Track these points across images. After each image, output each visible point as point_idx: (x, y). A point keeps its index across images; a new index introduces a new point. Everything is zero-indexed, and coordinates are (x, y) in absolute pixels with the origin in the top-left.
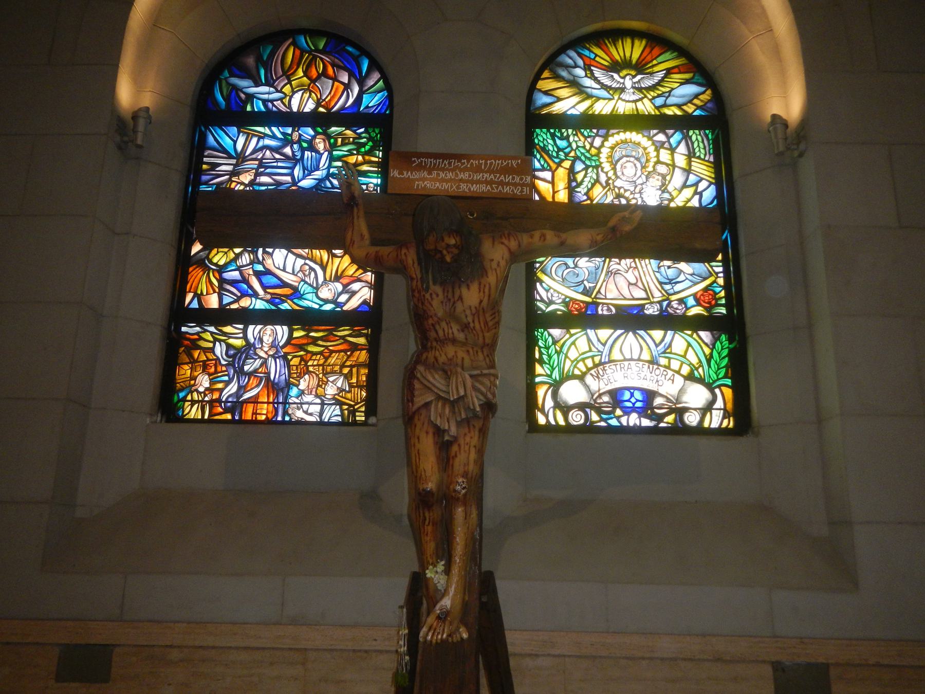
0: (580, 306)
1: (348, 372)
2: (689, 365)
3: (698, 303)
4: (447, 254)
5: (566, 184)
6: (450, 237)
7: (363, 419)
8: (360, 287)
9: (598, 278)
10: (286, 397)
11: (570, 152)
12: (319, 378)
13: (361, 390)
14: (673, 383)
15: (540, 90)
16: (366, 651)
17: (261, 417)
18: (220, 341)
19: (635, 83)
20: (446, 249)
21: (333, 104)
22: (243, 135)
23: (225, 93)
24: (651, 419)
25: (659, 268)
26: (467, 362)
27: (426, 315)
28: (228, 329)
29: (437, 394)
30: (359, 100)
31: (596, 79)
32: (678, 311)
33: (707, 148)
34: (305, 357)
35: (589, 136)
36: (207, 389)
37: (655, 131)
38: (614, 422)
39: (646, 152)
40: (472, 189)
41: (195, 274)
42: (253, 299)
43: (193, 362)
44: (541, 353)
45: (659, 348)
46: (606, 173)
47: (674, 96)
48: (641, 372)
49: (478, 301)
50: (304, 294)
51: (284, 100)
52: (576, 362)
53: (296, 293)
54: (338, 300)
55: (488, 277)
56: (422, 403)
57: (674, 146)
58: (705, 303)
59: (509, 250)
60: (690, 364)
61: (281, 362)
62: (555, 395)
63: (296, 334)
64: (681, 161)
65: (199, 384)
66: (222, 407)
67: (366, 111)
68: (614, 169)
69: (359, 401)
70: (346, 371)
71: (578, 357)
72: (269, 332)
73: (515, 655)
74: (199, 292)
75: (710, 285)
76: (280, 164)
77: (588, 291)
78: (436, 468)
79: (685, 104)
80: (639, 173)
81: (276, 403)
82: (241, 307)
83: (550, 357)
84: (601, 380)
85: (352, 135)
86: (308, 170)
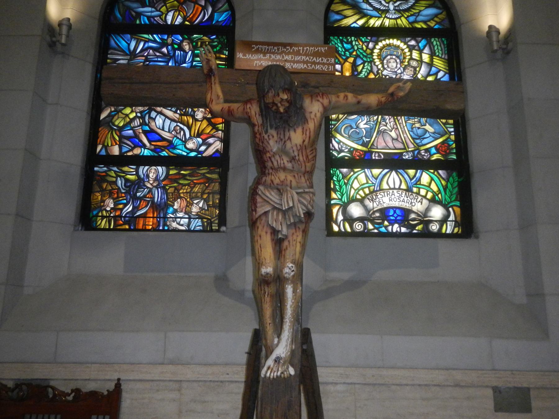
0: (360, 153)
1: (207, 197)
2: (432, 193)
3: (438, 151)
4: (281, 106)
6: (283, 93)
7: (217, 228)
8: (214, 141)
9: (372, 135)
10: (166, 214)
11: (353, 52)
12: (187, 201)
13: (215, 209)
14: (421, 204)
15: (333, 11)
16: (222, 382)
17: (149, 227)
18: (120, 177)
19: (395, 7)
20: (280, 103)
21: (194, 19)
22: (134, 40)
23: (122, 12)
24: (407, 228)
25: (412, 128)
26: (294, 184)
27: (265, 150)
28: (126, 169)
29: (273, 205)
30: (211, 17)
32: (425, 157)
33: (443, 50)
34: (178, 188)
35: (366, 42)
36: (112, 209)
37: (409, 39)
38: (383, 230)
39: (403, 52)
40: (294, 67)
41: (103, 131)
42: (143, 149)
43: (102, 191)
44: (335, 185)
45: (412, 182)
46: (377, 66)
47: (421, 15)
48: (400, 197)
49: (302, 140)
50: (176, 146)
51: (161, 17)
53: (171, 145)
54: (200, 150)
55: (308, 124)
56: (263, 212)
57: (422, 48)
58: (443, 151)
59: (323, 104)
60: (433, 192)
61: (162, 191)
62: (345, 212)
63: (172, 172)
64: (426, 58)
65: (107, 206)
66: (122, 221)
67: (217, 24)
68: (382, 63)
69: (214, 216)
70: (205, 196)
71: (359, 187)
72: (153, 171)
73: (323, 383)
74: (106, 144)
75: (446, 140)
76: (159, 59)
78: (272, 257)
79: (429, 21)
80: (399, 66)
81: (158, 218)
82: (134, 154)
83: (341, 187)
84: (375, 203)
85: (207, 40)
86: (178, 63)
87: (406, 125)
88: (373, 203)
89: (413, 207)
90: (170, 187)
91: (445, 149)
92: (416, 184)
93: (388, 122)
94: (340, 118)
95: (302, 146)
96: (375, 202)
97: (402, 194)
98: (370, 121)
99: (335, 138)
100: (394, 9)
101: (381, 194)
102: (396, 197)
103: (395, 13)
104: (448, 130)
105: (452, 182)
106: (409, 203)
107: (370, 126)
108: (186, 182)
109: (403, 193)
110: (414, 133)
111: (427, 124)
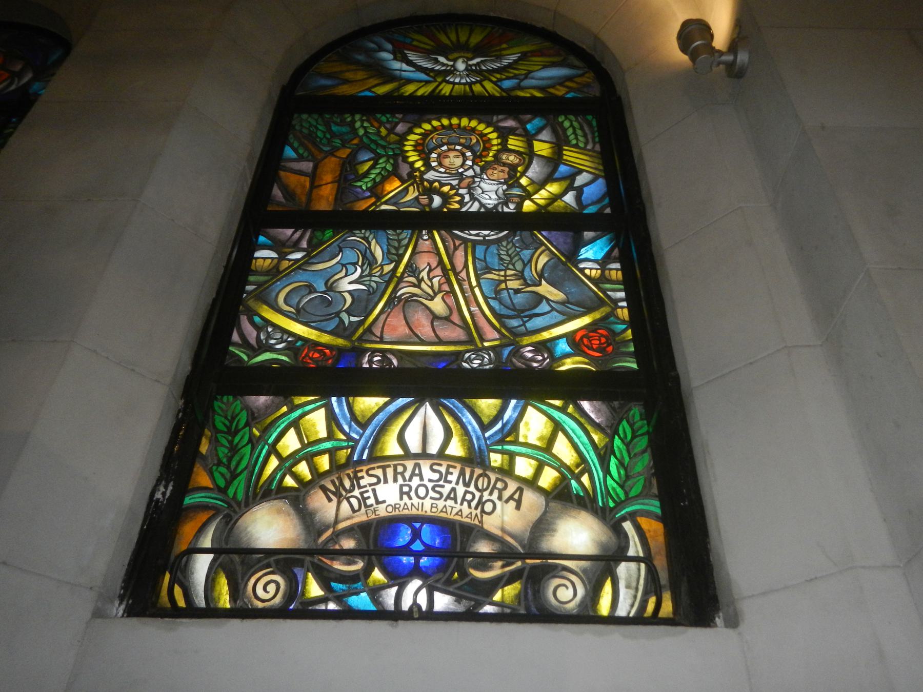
0: (325, 354)
14: (518, 507)
19: (471, 66)
24: (459, 598)
25: (497, 292)
31: (410, 63)
32: (535, 365)
38: (362, 601)
45: (487, 435)
48: (441, 483)
58: (594, 350)
60: (560, 466)
64: (542, 148)
75: (604, 318)
77: (345, 329)
80: (469, 163)
87: (479, 285)
88: (339, 503)
89: (485, 516)
91: (601, 344)
92: (502, 442)
93: (426, 278)
94: (281, 269)
96: (348, 499)
97: (448, 473)
98: (370, 275)
99: (251, 314)
100: (466, 69)
101: (371, 472)
102: (426, 482)
103: (468, 76)
104: (609, 297)
105: (629, 437)
106: (474, 504)
109: (451, 470)
110: (501, 303)
111: (543, 282)
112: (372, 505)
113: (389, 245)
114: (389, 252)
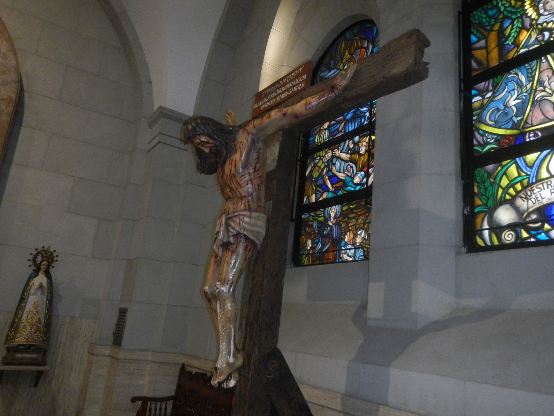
5: (497, 43)
9: (524, 110)
38: (542, 237)
41: (308, 184)
42: (328, 193)
52: (506, 190)
55: (236, 154)
70: (366, 226)
72: (333, 210)
77: (516, 125)
88: (528, 201)
90: (343, 222)
95: (230, 175)
98: (522, 93)
99: (478, 129)
101: (538, 187)
107: (522, 99)
108: (353, 215)
112: (540, 200)
113: (527, 73)
114: (528, 77)
